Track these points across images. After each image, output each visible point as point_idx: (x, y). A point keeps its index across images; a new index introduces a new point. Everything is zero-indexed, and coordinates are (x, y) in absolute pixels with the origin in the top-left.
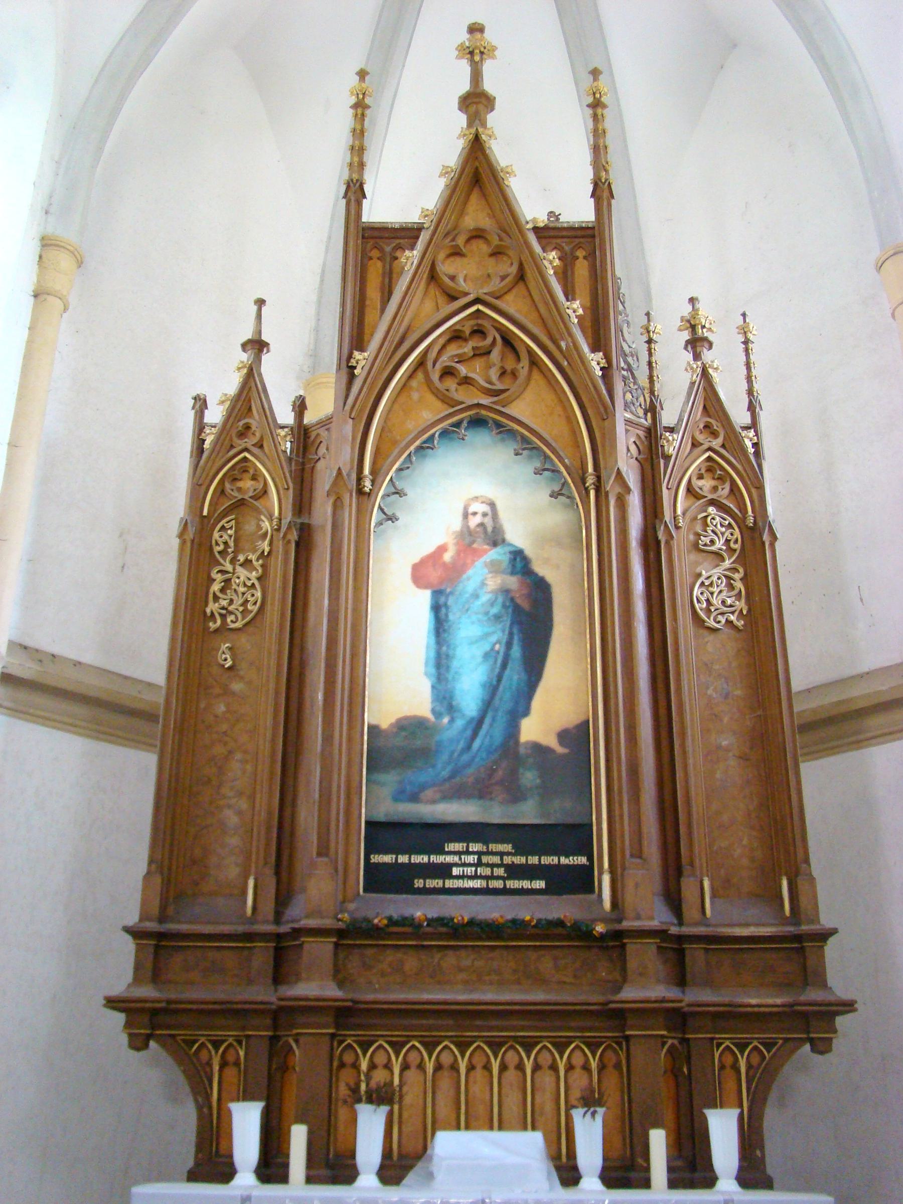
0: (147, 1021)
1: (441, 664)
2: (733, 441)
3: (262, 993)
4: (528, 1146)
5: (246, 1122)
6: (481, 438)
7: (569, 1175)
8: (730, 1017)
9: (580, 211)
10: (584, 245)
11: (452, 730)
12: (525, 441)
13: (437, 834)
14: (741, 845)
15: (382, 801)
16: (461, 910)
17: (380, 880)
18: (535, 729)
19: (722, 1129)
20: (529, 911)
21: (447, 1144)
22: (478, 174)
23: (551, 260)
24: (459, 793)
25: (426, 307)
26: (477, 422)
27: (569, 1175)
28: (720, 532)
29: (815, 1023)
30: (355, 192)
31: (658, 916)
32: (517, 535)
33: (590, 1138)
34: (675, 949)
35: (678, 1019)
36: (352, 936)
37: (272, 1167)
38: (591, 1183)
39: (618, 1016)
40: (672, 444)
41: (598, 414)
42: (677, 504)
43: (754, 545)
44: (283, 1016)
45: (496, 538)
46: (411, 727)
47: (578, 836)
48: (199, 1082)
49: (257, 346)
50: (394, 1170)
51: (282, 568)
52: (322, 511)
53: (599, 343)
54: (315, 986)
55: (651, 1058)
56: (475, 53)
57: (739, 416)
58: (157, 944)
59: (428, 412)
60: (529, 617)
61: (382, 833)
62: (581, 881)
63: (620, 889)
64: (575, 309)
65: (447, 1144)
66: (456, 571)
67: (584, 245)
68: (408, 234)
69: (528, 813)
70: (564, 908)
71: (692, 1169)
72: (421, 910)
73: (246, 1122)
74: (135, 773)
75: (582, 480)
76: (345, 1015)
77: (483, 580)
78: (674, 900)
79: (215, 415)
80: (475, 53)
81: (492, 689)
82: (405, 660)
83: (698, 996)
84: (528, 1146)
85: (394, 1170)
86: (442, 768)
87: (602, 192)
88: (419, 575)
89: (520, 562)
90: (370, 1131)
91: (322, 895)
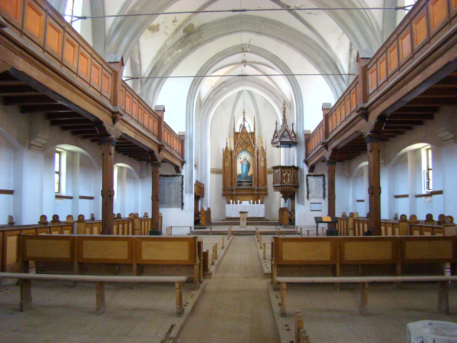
0: (224, 195)
1: (242, 170)
2: (264, 152)
3: (231, 193)
4: (248, 202)
5: (231, 201)
6: (245, 151)
7: (250, 203)
8: (261, 194)
9: (252, 131)
10: (253, 134)
11: (243, 175)
12: (249, 152)
13: (242, 182)
14: (263, 183)
15: (238, 180)
16: (244, 187)
17: (238, 185)
18: (249, 174)
19: (259, 201)
20: (248, 187)
21: (243, 202)
22: (244, 128)
23: (250, 136)
24: (243, 179)
25: (241, 140)
26: (244, 150)
27: (250, 203)
28: (263, 159)
29: (267, 194)
30: (234, 129)
31: (257, 188)
32: (248, 159)
33: (251, 201)
34: (258, 190)
35: (258, 194)
36: (237, 189)
37: (233, 203)
38: (251, 204)
39: (253, 194)
40: (259, 152)
41: (254, 150)
42: (260, 157)
43: (265, 160)
44: (232, 195)
45: (246, 159)
46: (240, 174)
47: (251, 182)
48: (227, 198)
49: (227, 143)
50: (240, 203)
51: (230, 163)
52: (233, 158)
53: (254, 144)
54: (234, 193)
55: (256, 197)
56: (244, 113)
57: (265, 149)
58: (224, 190)
59: (241, 149)
60: (248, 166)
61: (238, 182)
62: (251, 185)
63: (254, 186)
64: (252, 141)
65: (243, 202)
66: (243, 162)
67: (253, 134)
68: (238, 133)
69: (248, 180)
70: (250, 187)
71: (257, 203)
72: (241, 187)
73: (231, 201)
74: (221, 176)
75: (252, 155)
76: (236, 194)
77: (245, 163)
78: (258, 187)
79: (224, 150)
80: (244, 113)
81: (246, 171)
82: (240, 169)
83: (259, 193)
84: (248, 202)
85: (240, 203)
86: (242, 178)
87: (255, 129)
88: (240, 163)
89: (248, 162)
90: (239, 201)
91: (234, 187)
